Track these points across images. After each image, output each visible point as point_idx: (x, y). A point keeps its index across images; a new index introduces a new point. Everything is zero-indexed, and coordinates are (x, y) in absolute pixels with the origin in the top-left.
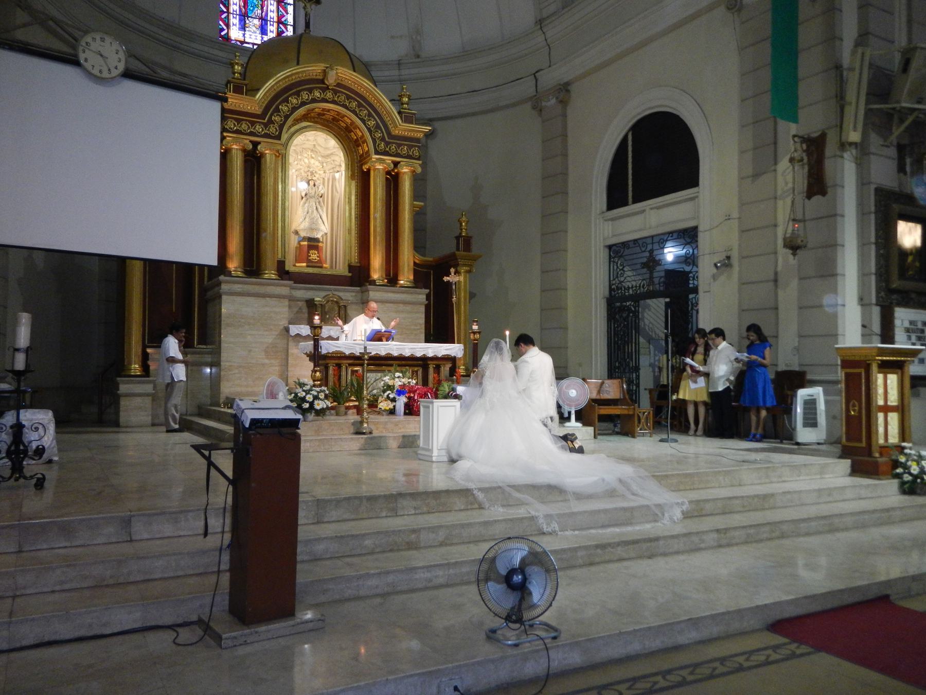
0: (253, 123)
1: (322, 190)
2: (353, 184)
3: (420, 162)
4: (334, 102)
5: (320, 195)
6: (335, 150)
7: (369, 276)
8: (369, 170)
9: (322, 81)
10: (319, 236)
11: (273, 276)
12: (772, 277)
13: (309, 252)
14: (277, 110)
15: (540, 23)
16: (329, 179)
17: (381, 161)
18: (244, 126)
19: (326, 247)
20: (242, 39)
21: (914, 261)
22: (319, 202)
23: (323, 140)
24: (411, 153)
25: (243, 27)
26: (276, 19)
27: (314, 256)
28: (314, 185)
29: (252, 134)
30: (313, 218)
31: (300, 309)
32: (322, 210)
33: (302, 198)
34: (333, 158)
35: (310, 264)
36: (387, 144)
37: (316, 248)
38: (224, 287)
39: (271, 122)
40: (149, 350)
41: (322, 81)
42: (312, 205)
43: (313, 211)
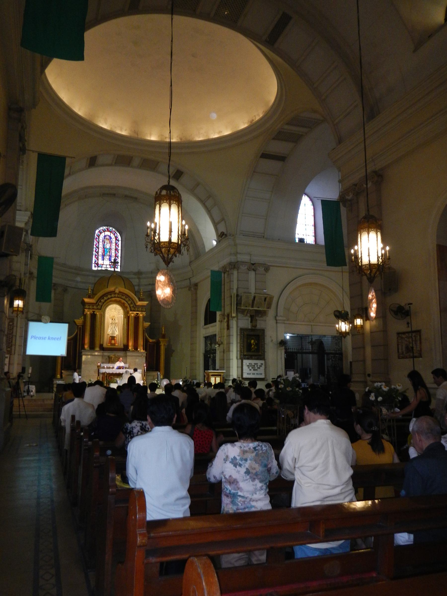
0: (93, 306)
1: (117, 321)
2: (126, 319)
3: (145, 312)
4: (118, 297)
7: (128, 348)
8: (129, 316)
9: (114, 292)
10: (115, 335)
11: (98, 349)
12: (223, 351)
14: (101, 301)
15: (191, 262)
17: (132, 313)
18: (91, 307)
20: (102, 263)
21: (254, 347)
22: (116, 325)
24: (142, 310)
25: (103, 260)
26: (114, 255)
27: (113, 342)
29: (93, 309)
31: (106, 358)
32: (116, 328)
35: (112, 344)
36: (134, 308)
37: (114, 339)
38: (83, 353)
39: (98, 305)
40: (63, 371)
41: (114, 292)
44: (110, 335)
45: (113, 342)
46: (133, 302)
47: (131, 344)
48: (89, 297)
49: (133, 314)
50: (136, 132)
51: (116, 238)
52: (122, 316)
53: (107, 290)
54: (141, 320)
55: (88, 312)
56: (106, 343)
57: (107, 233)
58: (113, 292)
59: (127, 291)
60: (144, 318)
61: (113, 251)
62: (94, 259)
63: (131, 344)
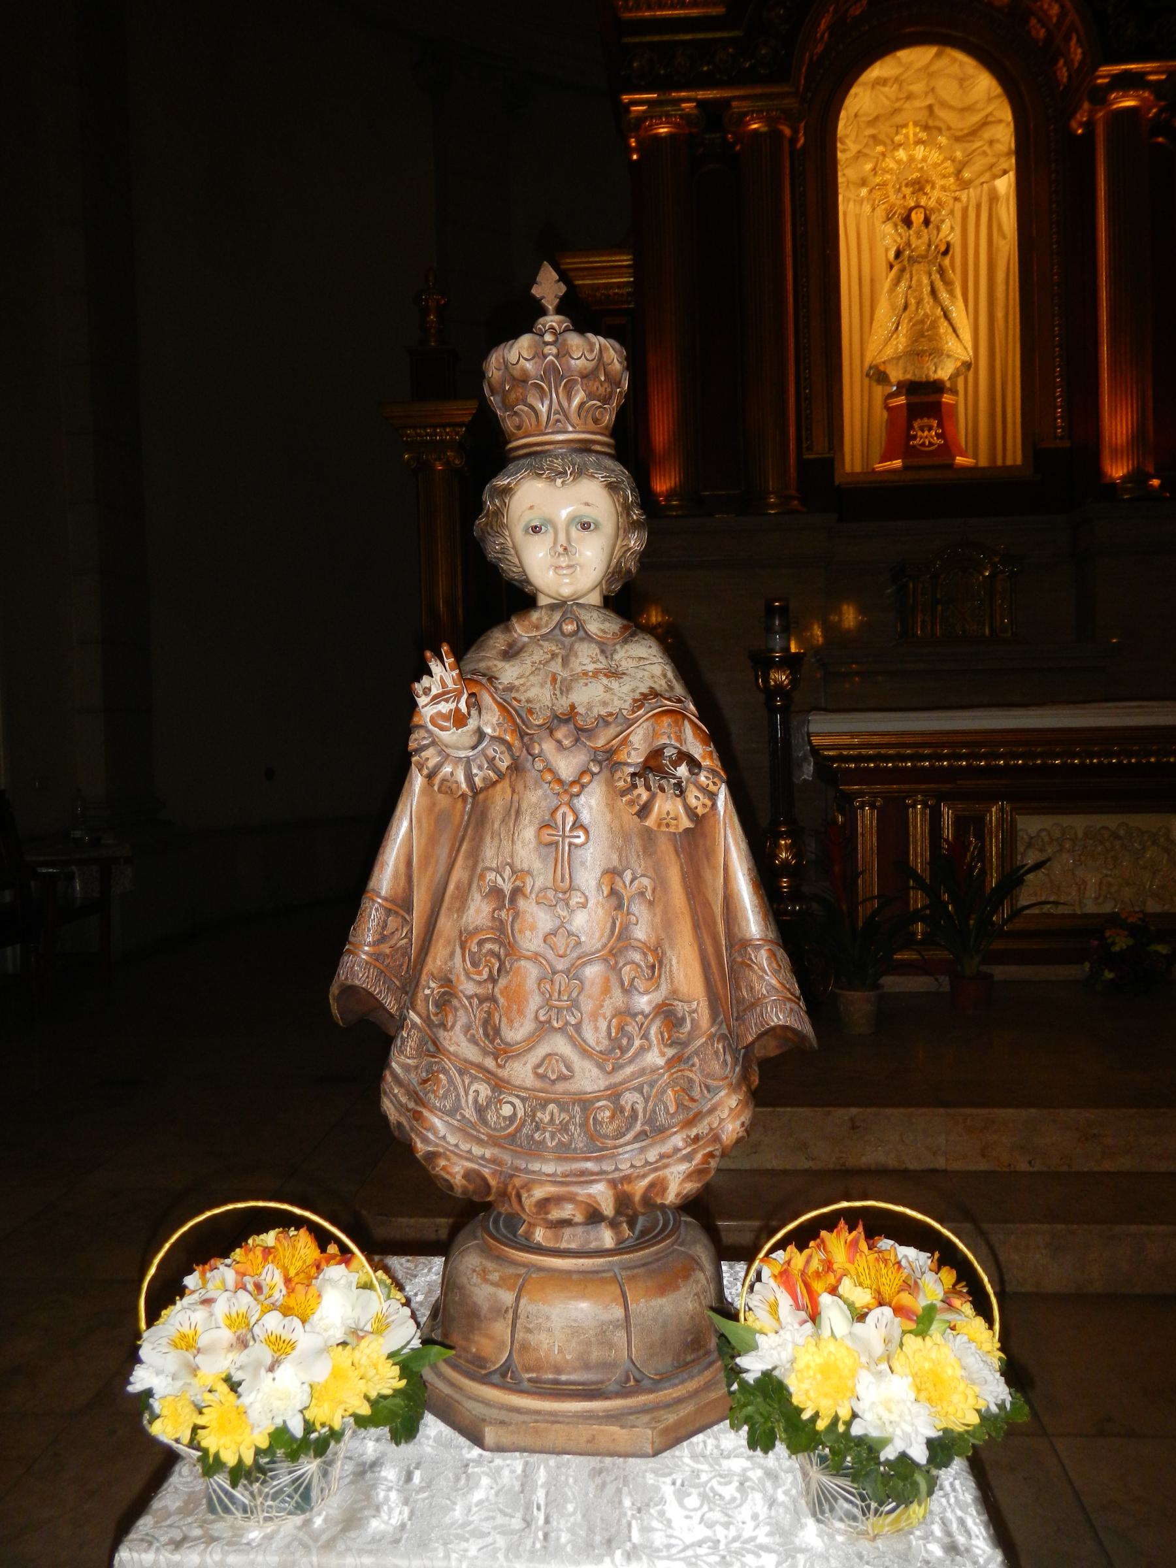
1: (949, 231)
5: (943, 248)
6: (989, 110)
10: (944, 372)
13: (911, 427)
16: (978, 206)
19: (956, 401)
23: (955, 84)
27: (927, 436)
28: (927, 222)
30: (922, 322)
32: (951, 293)
33: (891, 267)
34: (987, 134)
42: (919, 282)
43: (919, 302)
44: (896, 374)
45: (927, 436)
52: (1005, 185)
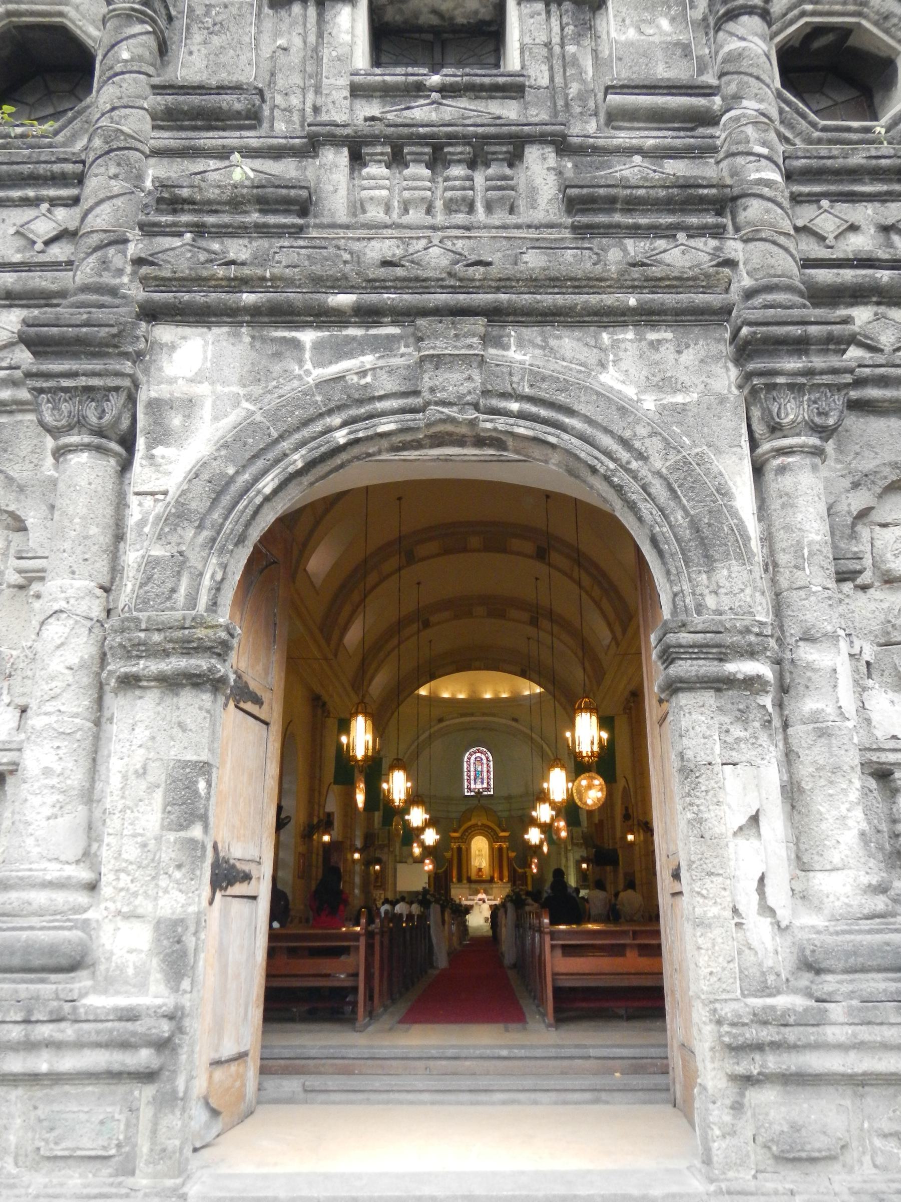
46: (496, 834)
47: (496, 875)
48: (455, 831)
49: (497, 845)
50: (474, 692)
51: (487, 758)
53: (470, 824)
54: (505, 851)
55: (454, 846)
56: (474, 876)
57: (478, 755)
58: (475, 825)
59: (489, 824)
60: (508, 849)
61: (485, 774)
62: (466, 783)
63: (496, 875)
